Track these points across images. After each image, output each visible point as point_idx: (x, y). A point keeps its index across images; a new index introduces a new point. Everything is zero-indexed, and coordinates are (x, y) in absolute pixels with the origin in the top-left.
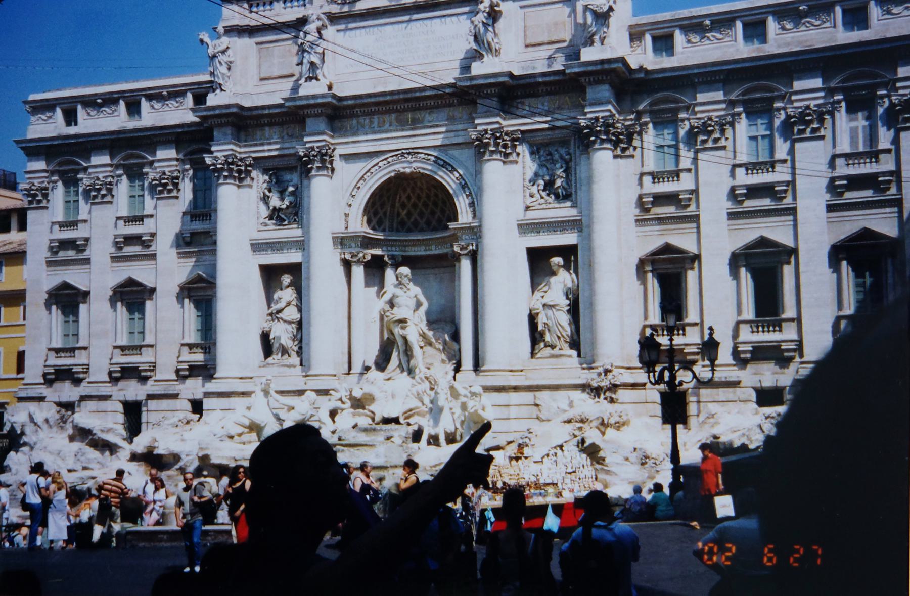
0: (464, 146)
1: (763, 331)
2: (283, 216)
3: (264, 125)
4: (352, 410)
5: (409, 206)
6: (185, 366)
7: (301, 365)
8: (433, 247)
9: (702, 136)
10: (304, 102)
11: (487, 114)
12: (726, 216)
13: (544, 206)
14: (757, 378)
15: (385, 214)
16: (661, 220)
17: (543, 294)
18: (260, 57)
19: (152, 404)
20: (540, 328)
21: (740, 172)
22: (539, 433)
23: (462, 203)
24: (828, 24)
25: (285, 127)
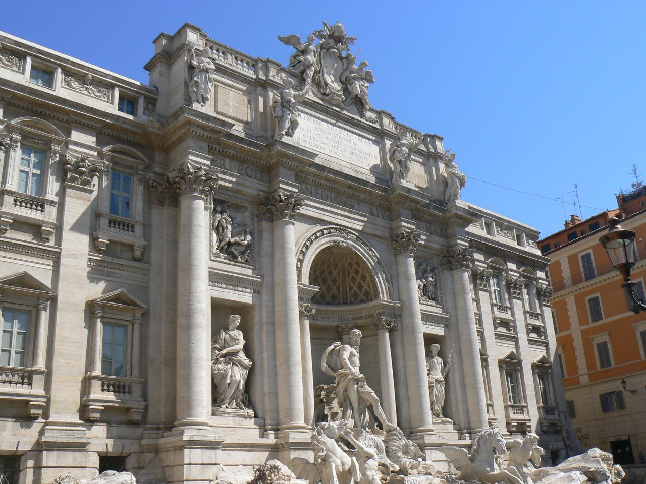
2: (236, 252)
7: (256, 417)
12: (494, 336)
13: (424, 302)
19: (49, 458)
21: (495, 308)
25: (245, 166)
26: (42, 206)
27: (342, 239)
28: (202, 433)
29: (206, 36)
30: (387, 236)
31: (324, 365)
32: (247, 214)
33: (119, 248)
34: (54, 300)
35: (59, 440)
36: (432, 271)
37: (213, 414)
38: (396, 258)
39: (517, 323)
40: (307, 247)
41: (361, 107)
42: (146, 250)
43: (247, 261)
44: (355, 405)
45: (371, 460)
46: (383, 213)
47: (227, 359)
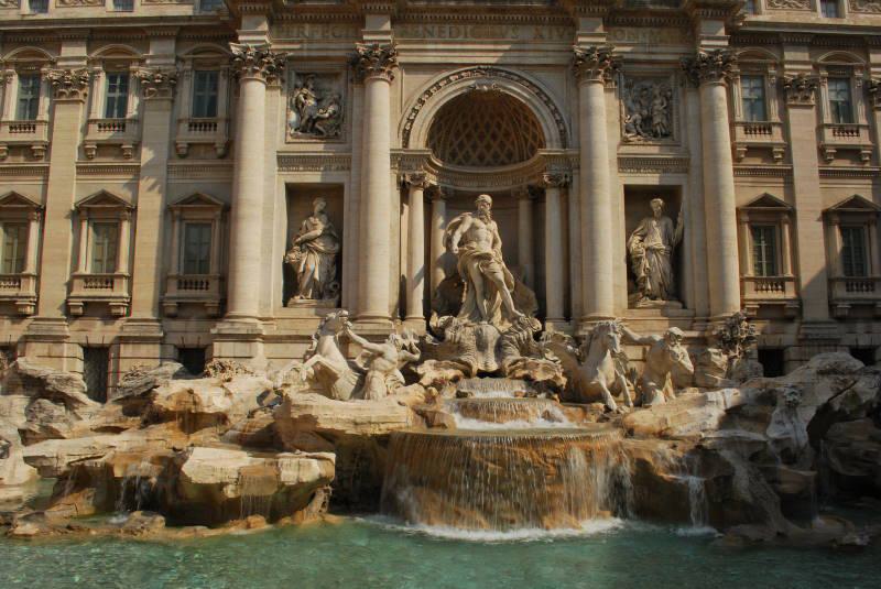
1: (857, 290)
2: (321, 128)
3: (303, 22)
4: (434, 361)
5: (463, 137)
6: (173, 303)
8: (488, 184)
9: (794, 91)
13: (642, 142)
14: (853, 337)
15: (439, 140)
16: (754, 172)
17: (639, 238)
19: (126, 350)
22: (802, 387)
23: (549, 129)
25: (331, 26)
26: (124, 126)
28: (237, 326)
32: (342, 81)
33: (202, 150)
34: (134, 211)
37: (285, 305)
38: (578, 90)
40: (422, 102)
43: (336, 134)
44: (479, 291)
45: (380, 359)
46: (561, 30)
47: (304, 247)
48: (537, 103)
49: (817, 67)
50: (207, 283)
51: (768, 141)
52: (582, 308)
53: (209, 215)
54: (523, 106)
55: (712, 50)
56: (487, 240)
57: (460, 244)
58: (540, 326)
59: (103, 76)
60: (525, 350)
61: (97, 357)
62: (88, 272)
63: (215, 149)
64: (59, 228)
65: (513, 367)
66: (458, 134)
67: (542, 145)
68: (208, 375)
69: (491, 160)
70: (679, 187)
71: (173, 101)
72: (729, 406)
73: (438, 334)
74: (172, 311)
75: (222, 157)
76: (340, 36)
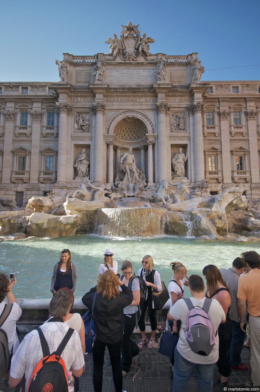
0: (150, 110)
2: (84, 128)
5: (125, 131)
6: (42, 179)
7: (89, 179)
8: (132, 145)
10: (97, 86)
11: (162, 99)
12: (229, 140)
18: (77, 75)
19: (29, 193)
20: (176, 170)
21: (233, 128)
23: (149, 128)
24: (254, 90)
25: (86, 98)
26: (27, 128)
27: (131, 114)
29: (72, 55)
30: (154, 107)
31: (119, 161)
32: (90, 115)
35: (30, 188)
36: (183, 118)
38: (158, 116)
39: (250, 132)
41: (145, 56)
42: (58, 134)
43: (88, 130)
47: (79, 162)
48: (145, 120)
49: (230, 108)
50: (52, 173)
51: (214, 131)
52: (158, 179)
53: (52, 154)
54: (142, 122)
55: (198, 102)
56: (131, 160)
57: (123, 161)
58: (146, 184)
59: (20, 113)
60: (141, 190)
61: (20, 194)
62: (17, 170)
63: (54, 135)
64: (8, 157)
65: (138, 195)
66: (124, 131)
67: (147, 133)
68: (47, 196)
69: (133, 139)
70: (187, 144)
71: (41, 121)
72: (200, 202)
73: (116, 186)
74: (42, 181)
75: (56, 137)
76: (88, 101)
